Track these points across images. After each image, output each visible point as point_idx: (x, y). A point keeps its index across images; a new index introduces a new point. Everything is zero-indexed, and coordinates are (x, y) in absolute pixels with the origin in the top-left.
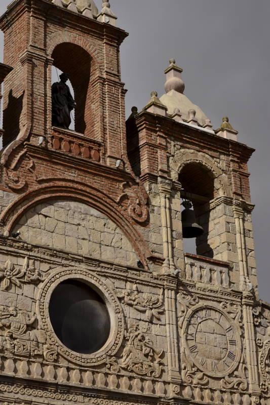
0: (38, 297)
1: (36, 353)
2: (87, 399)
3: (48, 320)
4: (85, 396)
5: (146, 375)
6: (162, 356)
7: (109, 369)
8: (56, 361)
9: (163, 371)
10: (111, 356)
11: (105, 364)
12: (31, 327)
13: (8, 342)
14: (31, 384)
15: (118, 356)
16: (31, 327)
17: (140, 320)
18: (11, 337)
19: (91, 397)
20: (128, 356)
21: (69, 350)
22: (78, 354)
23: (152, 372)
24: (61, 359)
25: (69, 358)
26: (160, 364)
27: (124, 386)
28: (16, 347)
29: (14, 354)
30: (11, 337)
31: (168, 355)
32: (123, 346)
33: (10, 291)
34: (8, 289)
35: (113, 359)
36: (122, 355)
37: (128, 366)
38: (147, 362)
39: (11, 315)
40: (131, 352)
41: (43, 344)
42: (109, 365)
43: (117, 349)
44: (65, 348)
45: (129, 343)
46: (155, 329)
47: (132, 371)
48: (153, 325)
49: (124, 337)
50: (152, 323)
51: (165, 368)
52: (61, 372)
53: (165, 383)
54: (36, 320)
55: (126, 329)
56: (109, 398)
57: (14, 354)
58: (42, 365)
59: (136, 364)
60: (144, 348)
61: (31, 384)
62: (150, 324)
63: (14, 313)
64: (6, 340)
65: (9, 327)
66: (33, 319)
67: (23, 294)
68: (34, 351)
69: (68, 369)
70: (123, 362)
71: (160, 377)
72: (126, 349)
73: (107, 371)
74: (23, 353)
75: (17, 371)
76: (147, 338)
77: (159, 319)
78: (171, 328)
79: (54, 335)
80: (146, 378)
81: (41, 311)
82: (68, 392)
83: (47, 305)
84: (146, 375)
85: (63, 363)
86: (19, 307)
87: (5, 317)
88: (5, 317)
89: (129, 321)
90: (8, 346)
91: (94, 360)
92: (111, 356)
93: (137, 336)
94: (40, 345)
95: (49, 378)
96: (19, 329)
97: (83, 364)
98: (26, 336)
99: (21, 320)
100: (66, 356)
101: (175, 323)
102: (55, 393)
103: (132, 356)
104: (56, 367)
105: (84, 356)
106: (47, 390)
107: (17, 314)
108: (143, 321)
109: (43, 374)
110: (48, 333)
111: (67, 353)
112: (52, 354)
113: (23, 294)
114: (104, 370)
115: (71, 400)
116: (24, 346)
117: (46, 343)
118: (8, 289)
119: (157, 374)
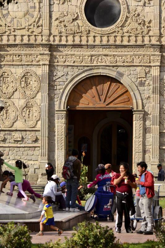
0: (79, 5)
1: (77, 31)
2: (104, 50)
3: (84, 15)
4: (103, 48)
5: (139, 34)
6: (150, 22)
7: (118, 33)
8: (89, 33)
9: (149, 31)
10: (118, 27)
11: (115, 32)
12: (74, 20)
13: (63, 29)
14: (74, 46)
15: (123, 26)
16: (74, 20)
17: (138, 6)
18: (65, 26)
19: (106, 48)
20: (128, 26)
21: (95, 28)
22: (100, 29)
23: (142, 32)
24: (91, 32)
25: (95, 31)
26: (148, 27)
27: (125, 41)
28: (67, 30)
29: (66, 33)
30: (65, 26)
31: (153, 22)
32: (126, 21)
33: (65, 4)
34: (63, 3)
35: (120, 28)
36: (125, 25)
37: (128, 31)
38: (139, 28)
39: (66, 16)
40: (130, 23)
41: (82, 26)
42: (117, 32)
43: (122, 23)
44: (93, 27)
45: (130, 19)
46: (147, 9)
47: (131, 33)
48: (146, 7)
49: (127, 16)
50: (145, 6)
51: (152, 29)
52: (91, 39)
53: (150, 36)
54: (78, 16)
55: (129, 12)
56: (116, 48)
57: (66, 33)
58: (81, 36)
59: (133, 29)
60: (138, 20)
61: (74, 46)
62: (144, 7)
63: (66, 15)
64: (62, 28)
65: (64, 21)
66: (76, 15)
67: (71, 5)
68: (76, 31)
69: (94, 37)
70: (125, 29)
71: (148, 34)
72: (128, 22)
73: (117, 35)
74: (71, 33)
75: (68, 41)
76: (141, 15)
77: (149, 4)
78: (156, 7)
79: (87, 22)
80: (139, 35)
81: (81, 11)
82: (94, 47)
83: (83, 8)
84: (139, 34)
85: (92, 34)
86: (69, 11)
87: (61, 17)
88: (61, 17)
89: (131, 8)
90: (63, 30)
91: (109, 31)
92: (118, 27)
93: (134, 15)
94: (80, 27)
95: (84, 42)
96: (69, 21)
97: (103, 33)
98: (72, 24)
99: (70, 18)
100: (93, 31)
101: (158, 4)
102: (87, 48)
103: (132, 25)
104: (87, 37)
105: (104, 29)
106: (83, 48)
107: (68, 15)
108: (140, 6)
109: (81, 41)
110: (84, 21)
111: (94, 29)
112: (86, 31)
113: (71, 5)
114: (114, 34)
115: (96, 51)
116: (71, 29)
117: (83, 26)
118: (63, 3)
119: (146, 31)
